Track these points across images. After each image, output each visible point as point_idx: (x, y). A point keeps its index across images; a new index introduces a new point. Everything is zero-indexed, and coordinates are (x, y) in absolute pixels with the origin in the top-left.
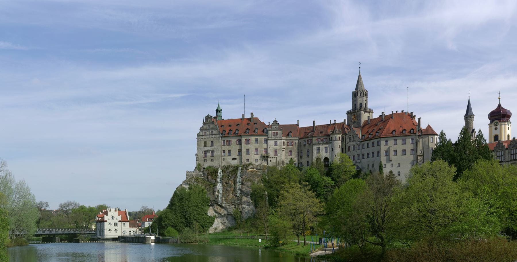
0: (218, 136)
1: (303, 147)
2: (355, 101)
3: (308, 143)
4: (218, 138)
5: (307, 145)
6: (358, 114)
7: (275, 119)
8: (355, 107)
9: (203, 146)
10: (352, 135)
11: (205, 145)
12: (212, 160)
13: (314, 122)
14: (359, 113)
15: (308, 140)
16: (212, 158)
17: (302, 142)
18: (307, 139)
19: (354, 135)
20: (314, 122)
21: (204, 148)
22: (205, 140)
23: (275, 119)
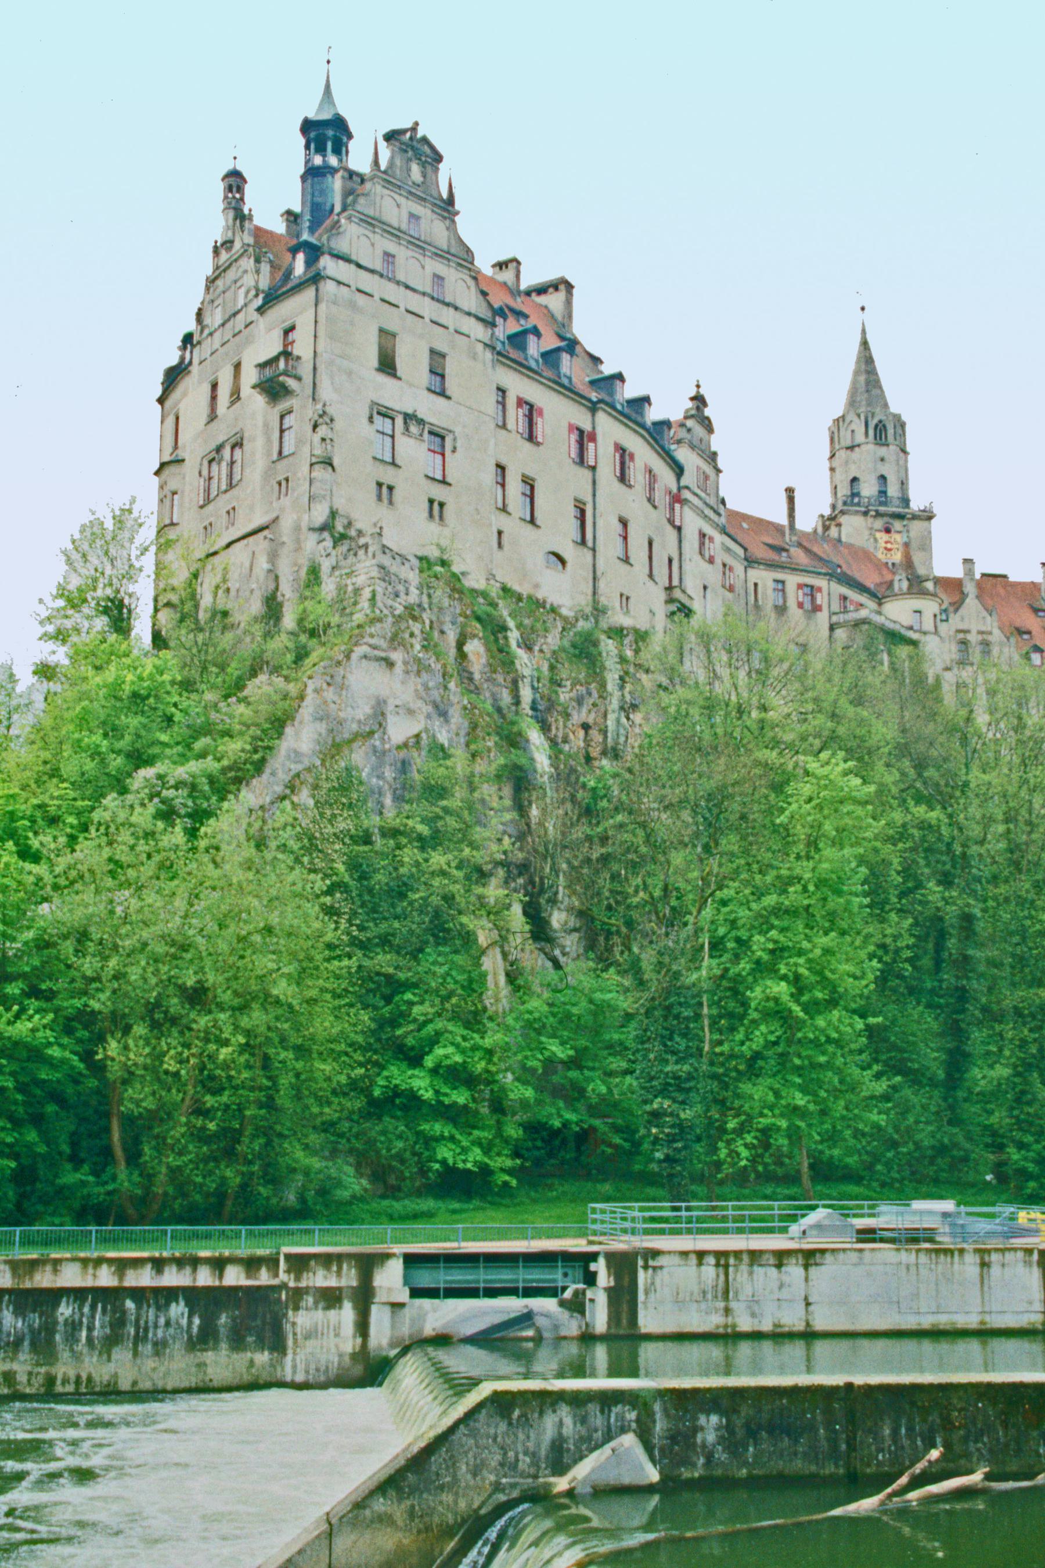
0: (479, 331)
1: (773, 615)
2: (882, 460)
3: (800, 605)
4: (480, 347)
5: (794, 612)
6: (912, 534)
7: (698, 386)
8: (883, 493)
9: (375, 363)
10: (974, 631)
11: (387, 365)
12: (436, 509)
13: (790, 492)
14: (916, 526)
15: (800, 586)
16: (438, 492)
17: (765, 586)
18: (792, 580)
19: (990, 633)
20: (790, 492)
21: (383, 379)
22: (393, 321)
23: (698, 386)
